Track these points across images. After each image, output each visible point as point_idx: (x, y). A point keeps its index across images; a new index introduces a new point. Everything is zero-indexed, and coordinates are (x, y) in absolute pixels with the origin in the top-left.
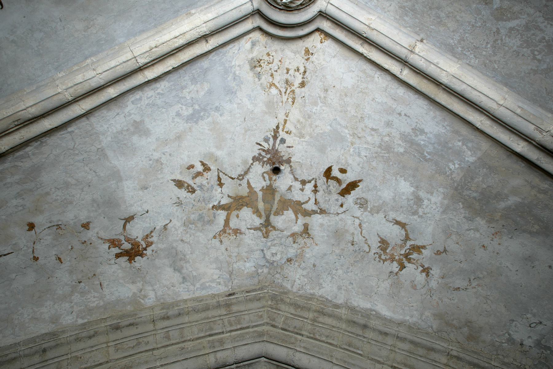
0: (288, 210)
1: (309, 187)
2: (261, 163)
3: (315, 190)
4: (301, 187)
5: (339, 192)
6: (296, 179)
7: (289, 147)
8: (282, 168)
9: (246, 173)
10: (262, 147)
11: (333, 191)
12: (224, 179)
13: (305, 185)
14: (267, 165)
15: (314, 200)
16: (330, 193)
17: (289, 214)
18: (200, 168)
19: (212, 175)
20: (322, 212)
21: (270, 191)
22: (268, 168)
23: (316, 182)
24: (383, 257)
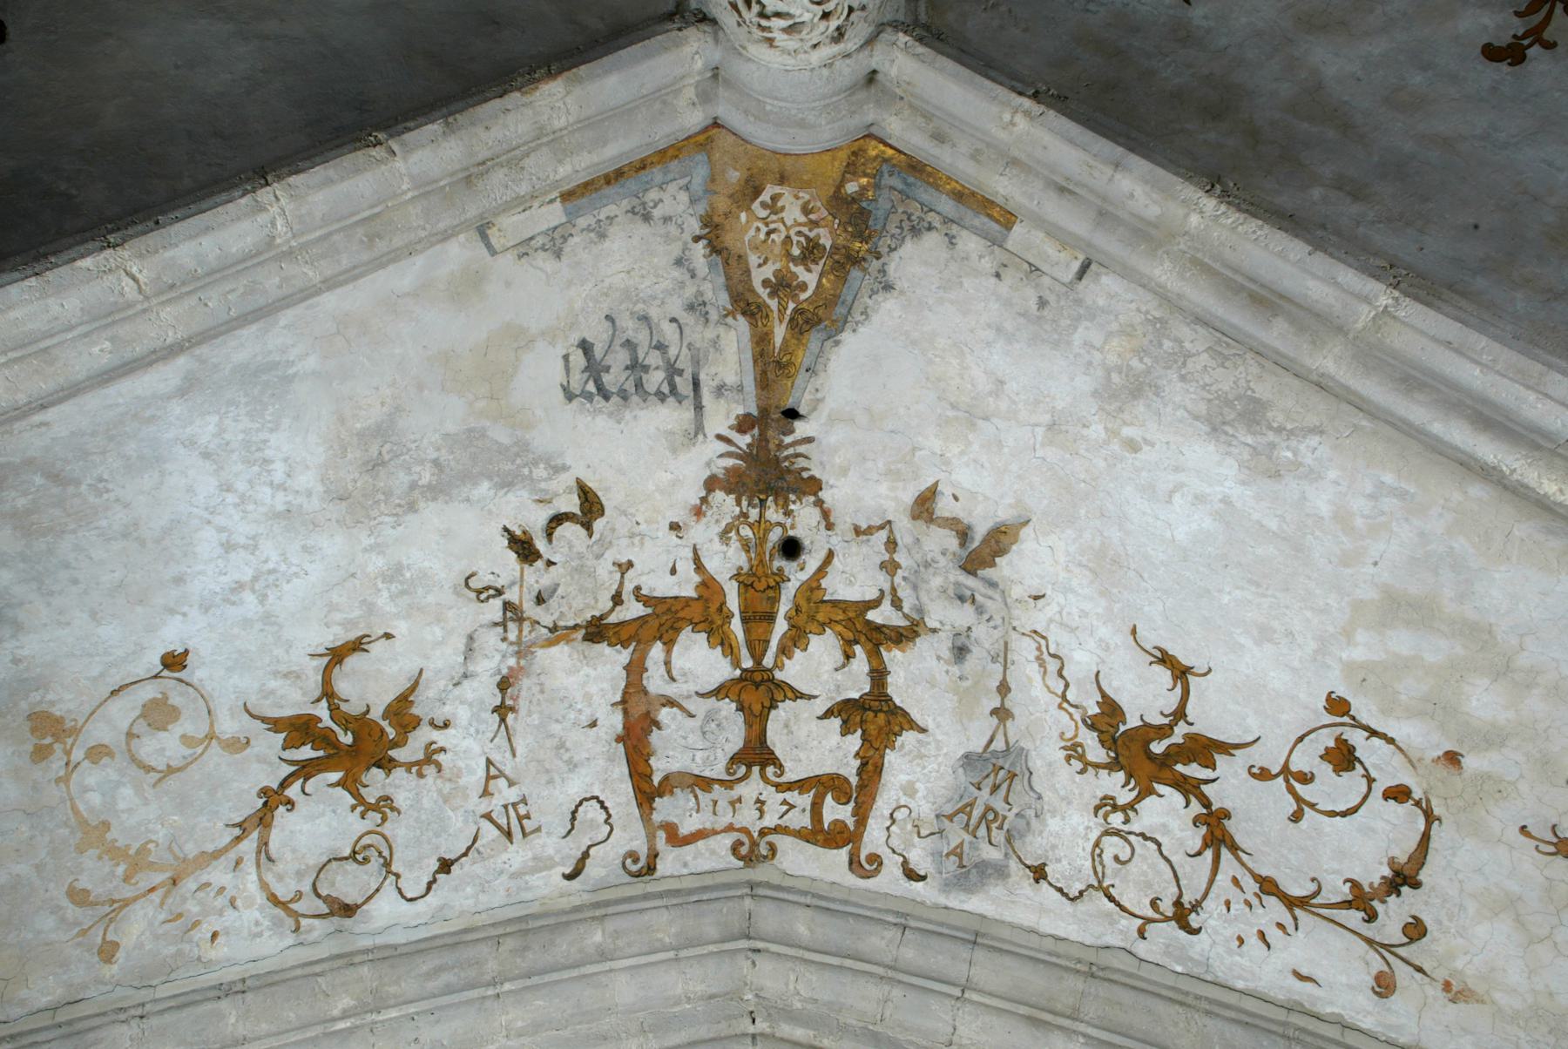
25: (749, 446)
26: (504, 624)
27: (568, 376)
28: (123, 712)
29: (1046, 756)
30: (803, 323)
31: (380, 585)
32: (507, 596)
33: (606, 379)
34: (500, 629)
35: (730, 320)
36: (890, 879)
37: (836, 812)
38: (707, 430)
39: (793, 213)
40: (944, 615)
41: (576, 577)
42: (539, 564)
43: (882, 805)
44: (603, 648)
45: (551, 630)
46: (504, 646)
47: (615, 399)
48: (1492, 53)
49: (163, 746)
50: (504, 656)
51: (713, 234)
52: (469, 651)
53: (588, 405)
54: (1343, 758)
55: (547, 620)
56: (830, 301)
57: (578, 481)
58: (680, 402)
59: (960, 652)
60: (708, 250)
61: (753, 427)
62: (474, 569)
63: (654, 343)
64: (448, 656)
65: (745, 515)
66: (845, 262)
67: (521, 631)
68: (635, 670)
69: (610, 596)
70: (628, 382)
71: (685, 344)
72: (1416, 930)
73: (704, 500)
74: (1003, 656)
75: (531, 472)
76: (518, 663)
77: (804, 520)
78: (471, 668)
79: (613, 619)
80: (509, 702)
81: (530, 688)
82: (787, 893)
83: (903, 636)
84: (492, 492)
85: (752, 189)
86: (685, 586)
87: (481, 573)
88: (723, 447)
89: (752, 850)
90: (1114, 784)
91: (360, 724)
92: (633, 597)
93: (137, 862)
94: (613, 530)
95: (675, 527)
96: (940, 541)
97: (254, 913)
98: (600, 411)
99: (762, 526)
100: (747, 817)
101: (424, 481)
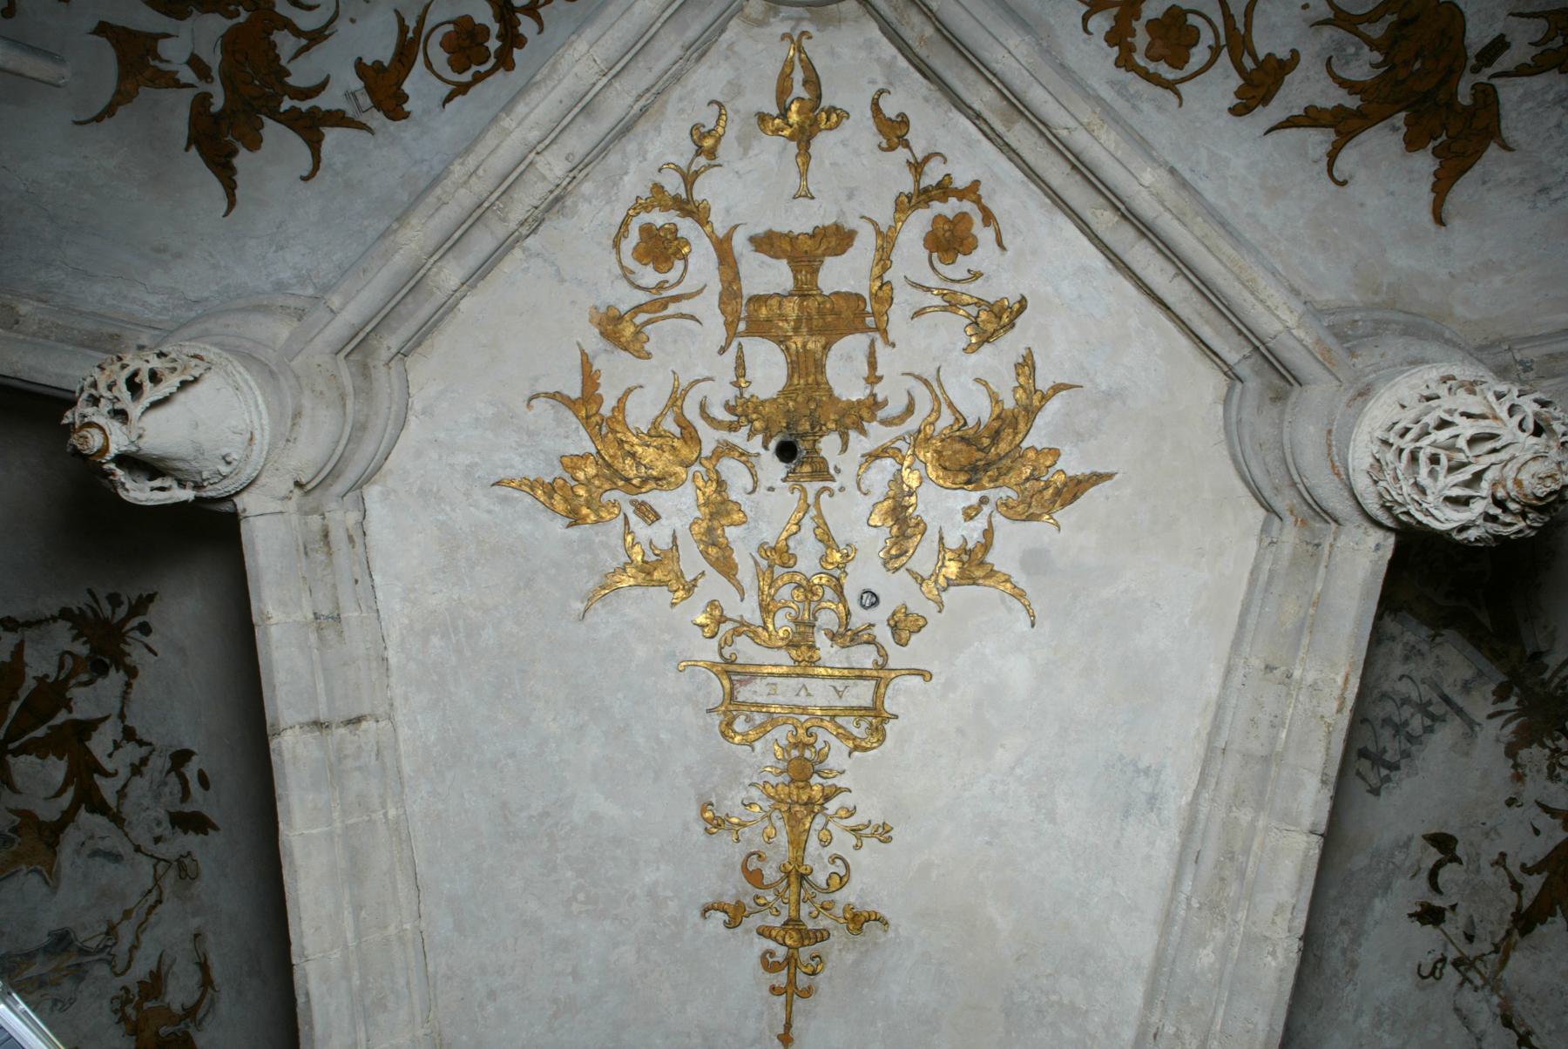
0: (61, 758)
1: (131, 752)
2: (75, 632)
3: (136, 770)
4: (119, 739)
5: (172, 810)
6: (122, 716)
7: (151, 650)
8: (112, 672)
9: (29, 624)
10: (95, 605)
11: (163, 800)
13: (128, 741)
14: (85, 643)
15: (122, 783)
16: (157, 797)
17: (57, 769)
20: (118, 819)
21: (53, 695)
23: (151, 753)
24: (130, 1010)
25: (1518, 704)
26: (1466, 979)
27: (1367, 782)
31: (1378, 1034)
32: (1450, 957)
33: (1388, 757)
34: (1467, 985)
35: (1438, 639)
38: (1478, 720)
41: (1477, 899)
42: (1448, 914)
44: (1541, 930)
45: (1496, 951)
46: (1480, 994)
47: (1403, 762)
50: (1488, 1001)
52: (1465, 1019)
53: (1391, 785)
55: (1487, 948)
57: (1425, 837)
58: (1444, 721)
60: (1392, 616)
61: (1512, 689)
62: (1417, 962)
63: (1399, 703)
65: (1558, 750)
67: (1479, 973)
69: (1509, 890)
70: (1402, 745)
71: (1419, 683)
73: (1516, 766)
75: (1393, 863)
76: (1500, 996)
78: (1477, 1031)
79: (1526, 903)
80: (1522, 1030)
81: (1523, 1007)
84: (1384, 902)
87: (1423, 961)
88: (1499, 721)
92: (1525, 876)
94: (1471, 844)
95: (1510, 802)
98: (1401, 780)
101: (1347, 942)
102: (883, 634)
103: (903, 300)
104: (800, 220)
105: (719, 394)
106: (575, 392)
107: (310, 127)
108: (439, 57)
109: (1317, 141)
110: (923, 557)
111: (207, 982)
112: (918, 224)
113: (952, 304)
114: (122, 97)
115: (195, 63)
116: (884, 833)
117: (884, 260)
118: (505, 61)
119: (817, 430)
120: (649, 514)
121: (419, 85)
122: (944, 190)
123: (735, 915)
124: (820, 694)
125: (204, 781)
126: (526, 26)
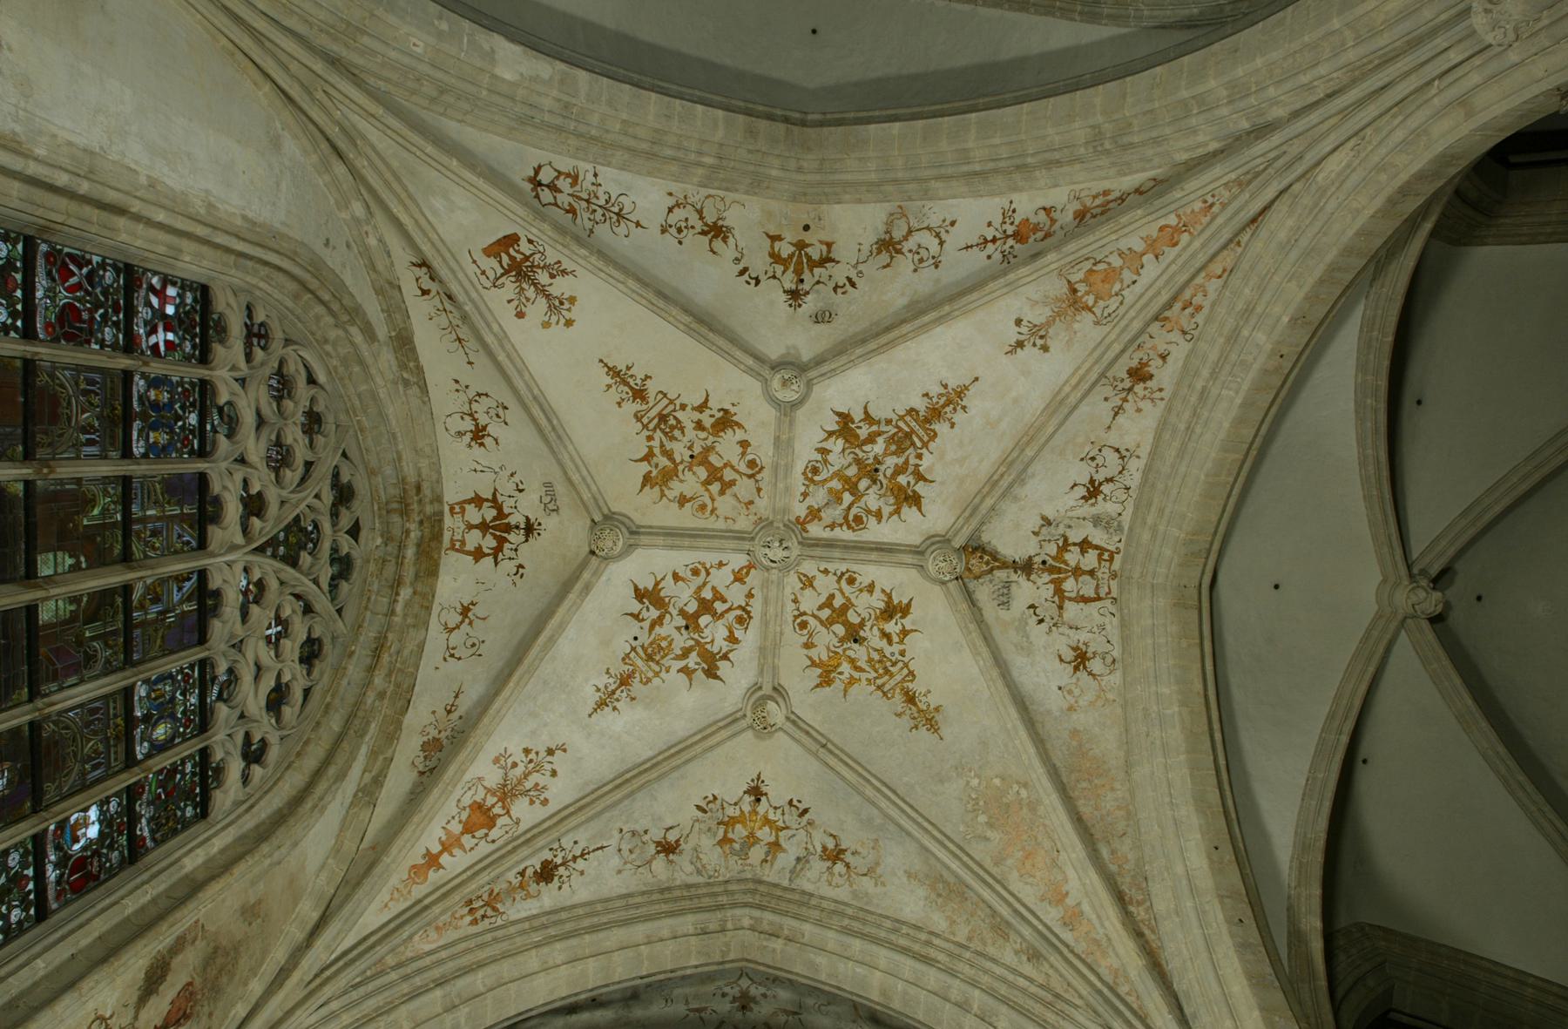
1: (779, 812)
12: (725, 805)
17: (767, 829)
18: (711, 798)
19: (718, 802)
20: (787, 828)
22: (753, 798)
28: (1068, 697)
29: (1094, 510)
30: (995, 559)
36: (1121, 545)
37: (1106, 556)
39: (974, 561)
40: (1061, 530)
43: (1105, 546)
48: (952, 427)
49: (1077, 692)
51: (977, 578)
54: (1093, 459)
56: (991, 554)
59: (1070, 527)
64: (1064, 639)
66: (984, 551)
68: (1070, 599)
72: (1127, 450)
74: (1071, 518)
77: (1038, 560)
82: (1122, 569)
83: (1066, 540)
85: (969, 570)
86: (1052, 587)
89: (1114, 576)
90: (1100, 498)
91: (1076, 658)
93: (1098, 697)
96: (1044, 530)
97: (1111, 677)
99: (1039, 569)
100: (1106, 576)
102: (900, 658)
103: (851, 596)
104: (823, 599)
105: (835, 641)
106: (809, 663)
107: (725, 657)
108: (737, 626)
109: (895, 517)
110: (895, 639)
111: (834, 837)
112: (843, 583)
113: (861, 590)
114: (691, 680)
115: (697, 663)
116: (929, 692)
117: (843, 593)
118: (750, 618)
119: (857, 633)
120: (841, 673)
121: (738, 634)
122: (843, 574)
123: (916, 727)
124: (898, 678)
125: (799, 801)
126: (749, 608)
